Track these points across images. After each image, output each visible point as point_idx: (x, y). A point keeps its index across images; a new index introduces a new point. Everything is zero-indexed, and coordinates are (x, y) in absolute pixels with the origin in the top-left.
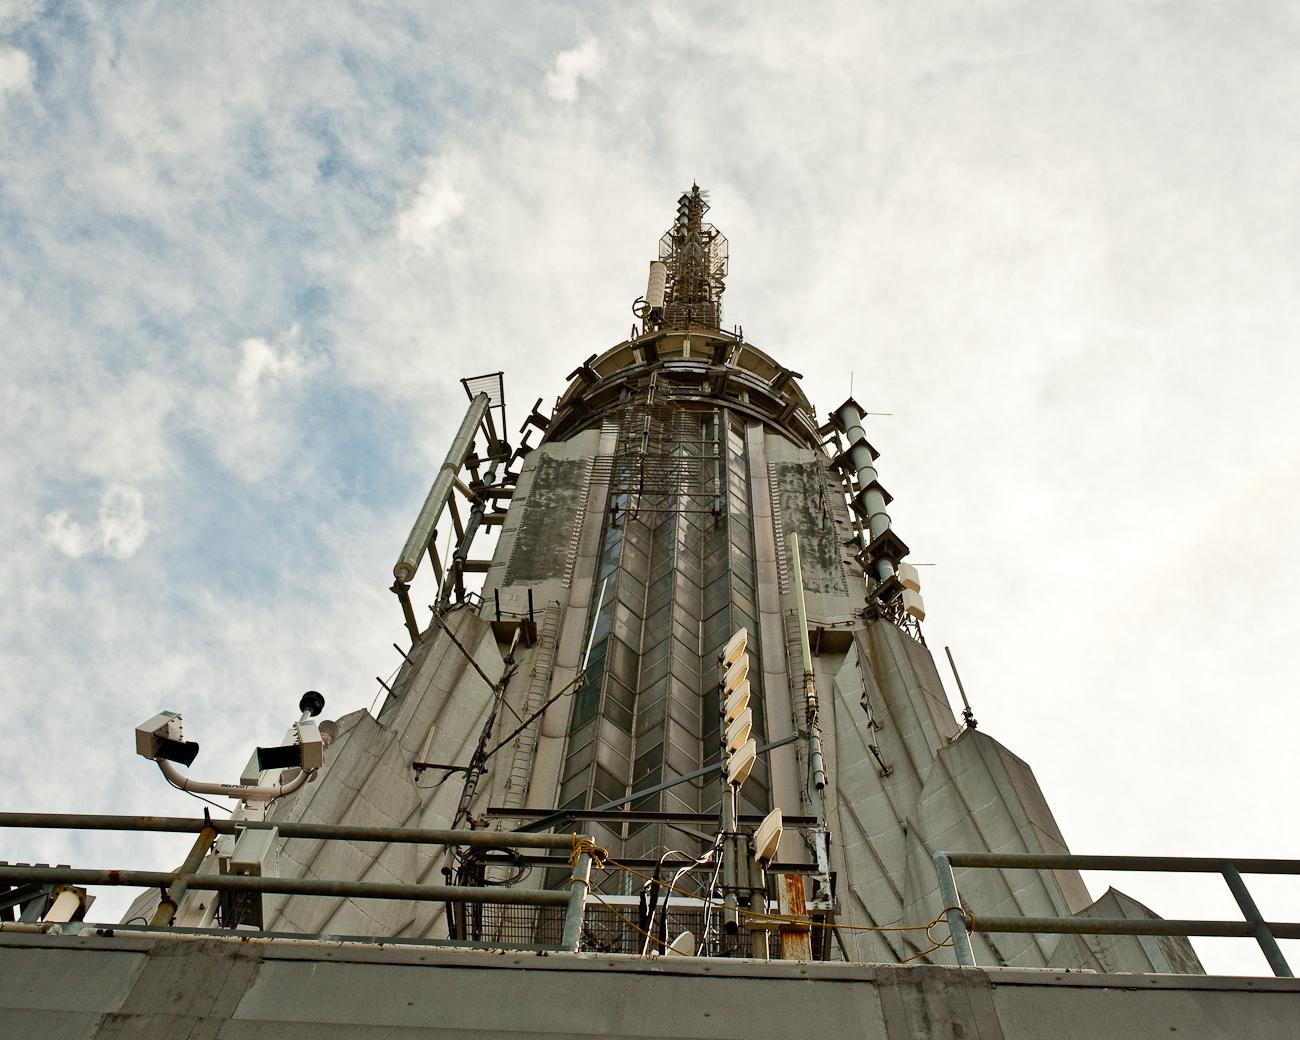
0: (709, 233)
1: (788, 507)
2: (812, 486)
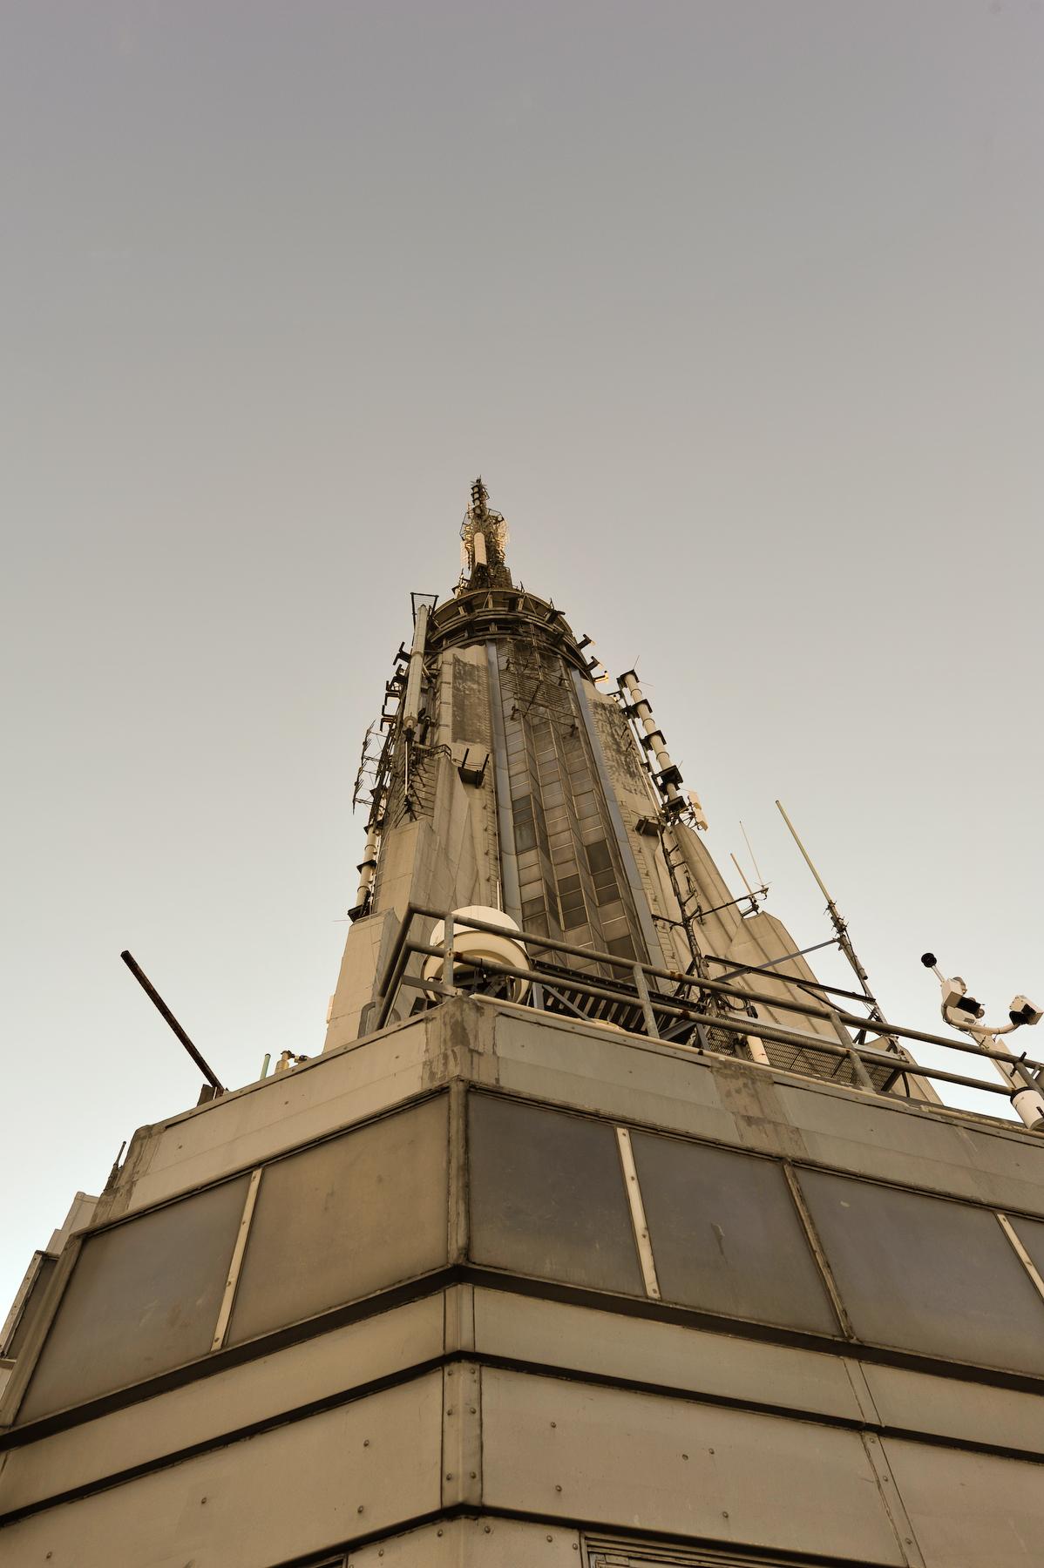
0: (497, 518)
1: (603, 732)
2: (613, 720)
